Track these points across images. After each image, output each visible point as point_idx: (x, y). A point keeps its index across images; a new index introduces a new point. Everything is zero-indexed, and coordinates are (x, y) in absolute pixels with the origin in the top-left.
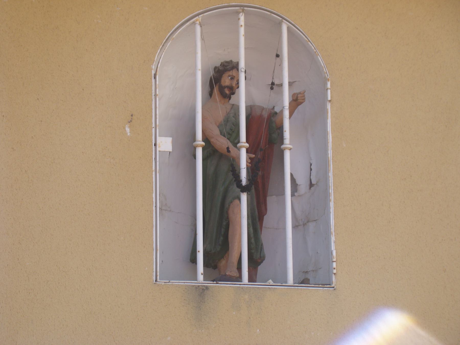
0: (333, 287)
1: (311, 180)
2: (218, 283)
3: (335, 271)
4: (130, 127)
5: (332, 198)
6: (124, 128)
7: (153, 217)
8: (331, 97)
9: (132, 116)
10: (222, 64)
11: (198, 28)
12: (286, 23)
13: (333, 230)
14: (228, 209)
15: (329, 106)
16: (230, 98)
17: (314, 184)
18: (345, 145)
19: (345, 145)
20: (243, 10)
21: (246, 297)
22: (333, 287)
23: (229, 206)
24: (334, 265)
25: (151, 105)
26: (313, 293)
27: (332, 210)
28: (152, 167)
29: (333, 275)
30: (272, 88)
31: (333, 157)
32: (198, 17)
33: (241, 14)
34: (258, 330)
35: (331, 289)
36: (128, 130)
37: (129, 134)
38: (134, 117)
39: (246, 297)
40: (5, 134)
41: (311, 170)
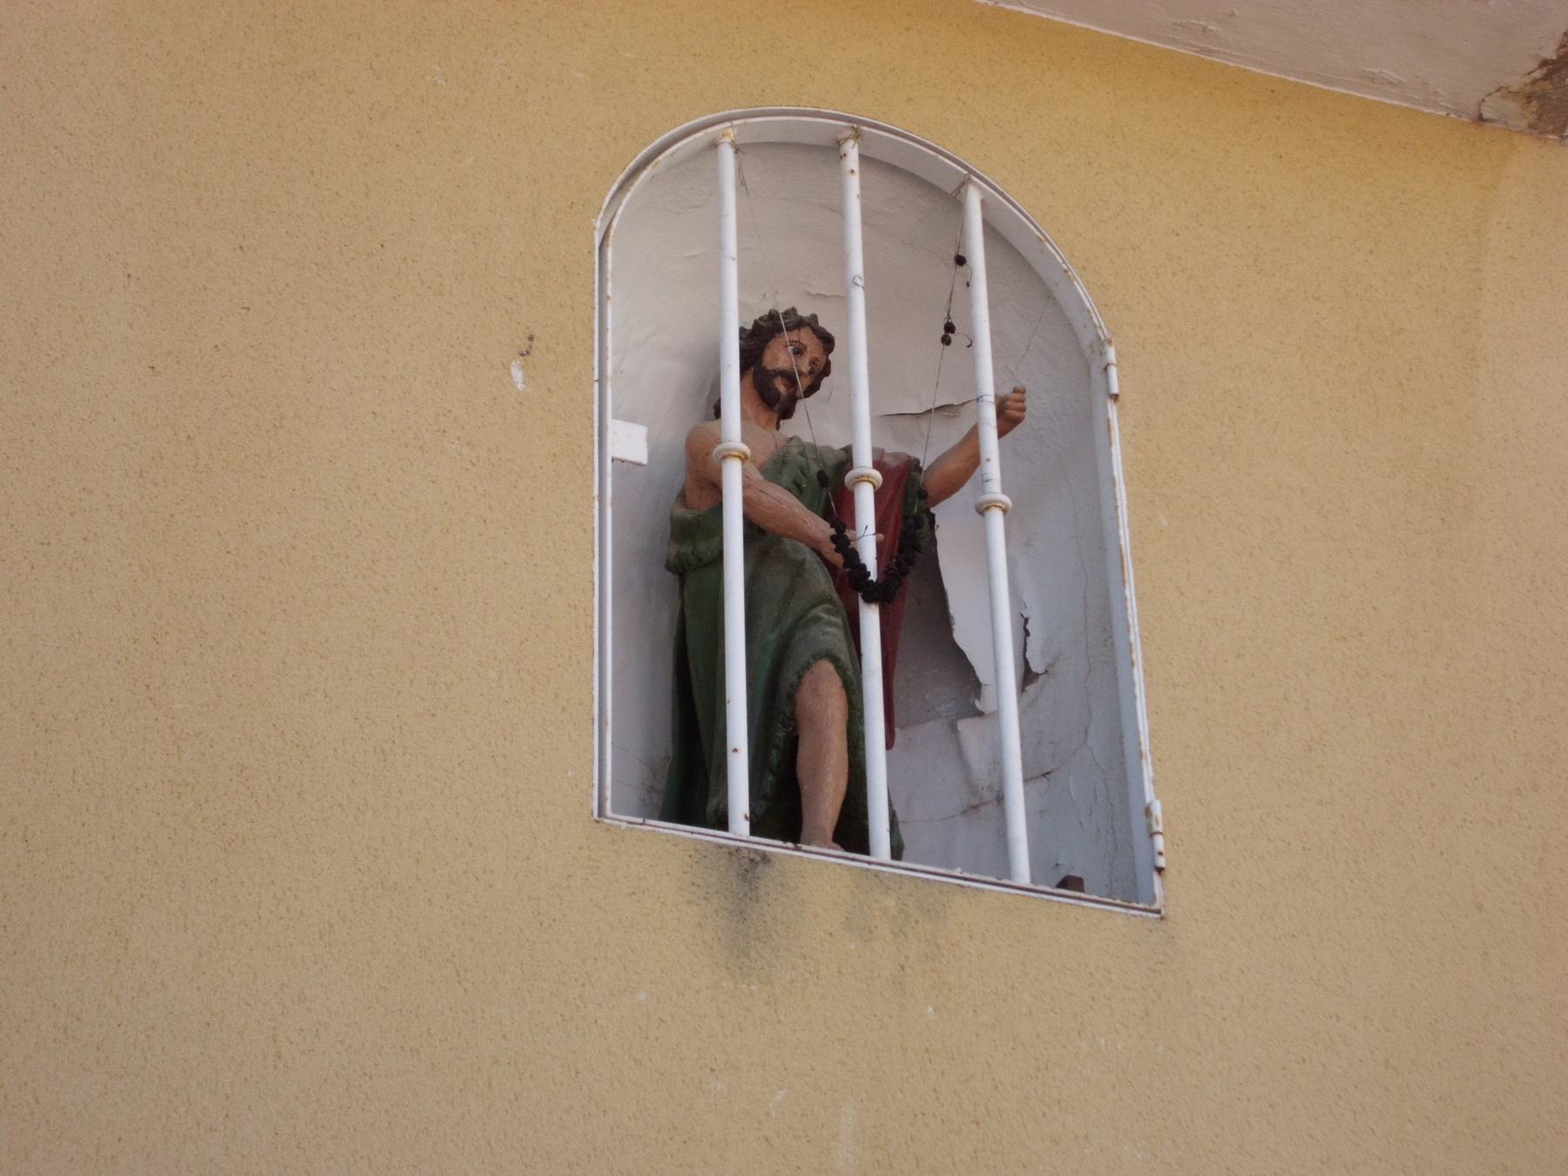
0: (1158, 912)
1: (1026, 662)
2: (799, 849)
3: (1161, 862)
4: (522, 367)
5: (1137, 656)
6: (507, 368)
7: (592, 627)
8: (1120, 387)
9: (531, 338)
10: (773, 316)
11: (728, 156)
12: (980, 187)
13: (1145, 746)
14: (796, 687)
15: (1113, 411)
16: (787, 413)
17: (1037, 675)
18: (1164, 522)
19: (1164, 522)
20: (858, 135)
21: (891, 902)
22: (1158, 912)
23: (800, 677)
24: (1159, 843)
25: (591, 320)
26: (1093, 924)
27: (1140, 690)
28: (590, 487)
29: (1156, 876)
30: (946, 341)
31: (1133, 547)
32: (728, 124)
33: (851, 143)
34: (930, 1009)
35: (1151, 915)
36: (517, 374)
37: (520, 386)
38: (535, 343)
39: (891, 902)
40: (131, 326)
41: (1027, 633)
